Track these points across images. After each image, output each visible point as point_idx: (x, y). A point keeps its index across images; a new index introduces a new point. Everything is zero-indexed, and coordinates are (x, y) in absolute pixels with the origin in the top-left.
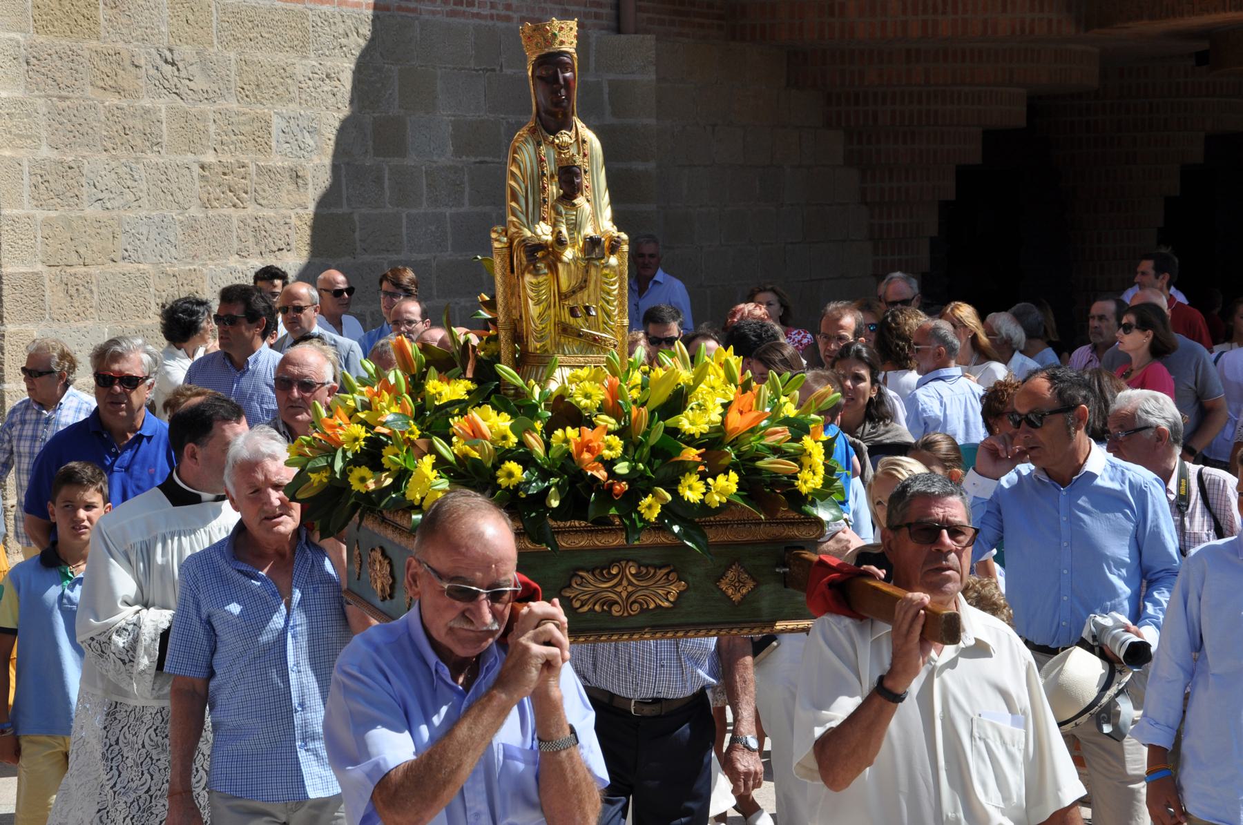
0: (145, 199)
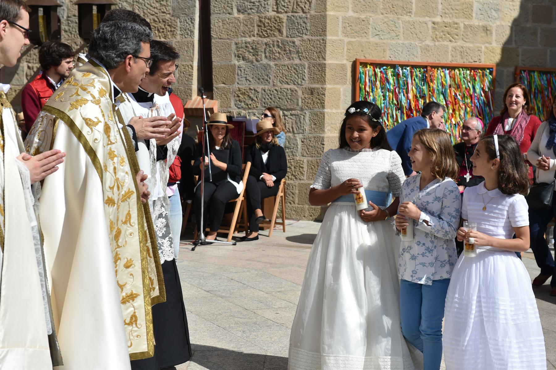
0: (401, 36)
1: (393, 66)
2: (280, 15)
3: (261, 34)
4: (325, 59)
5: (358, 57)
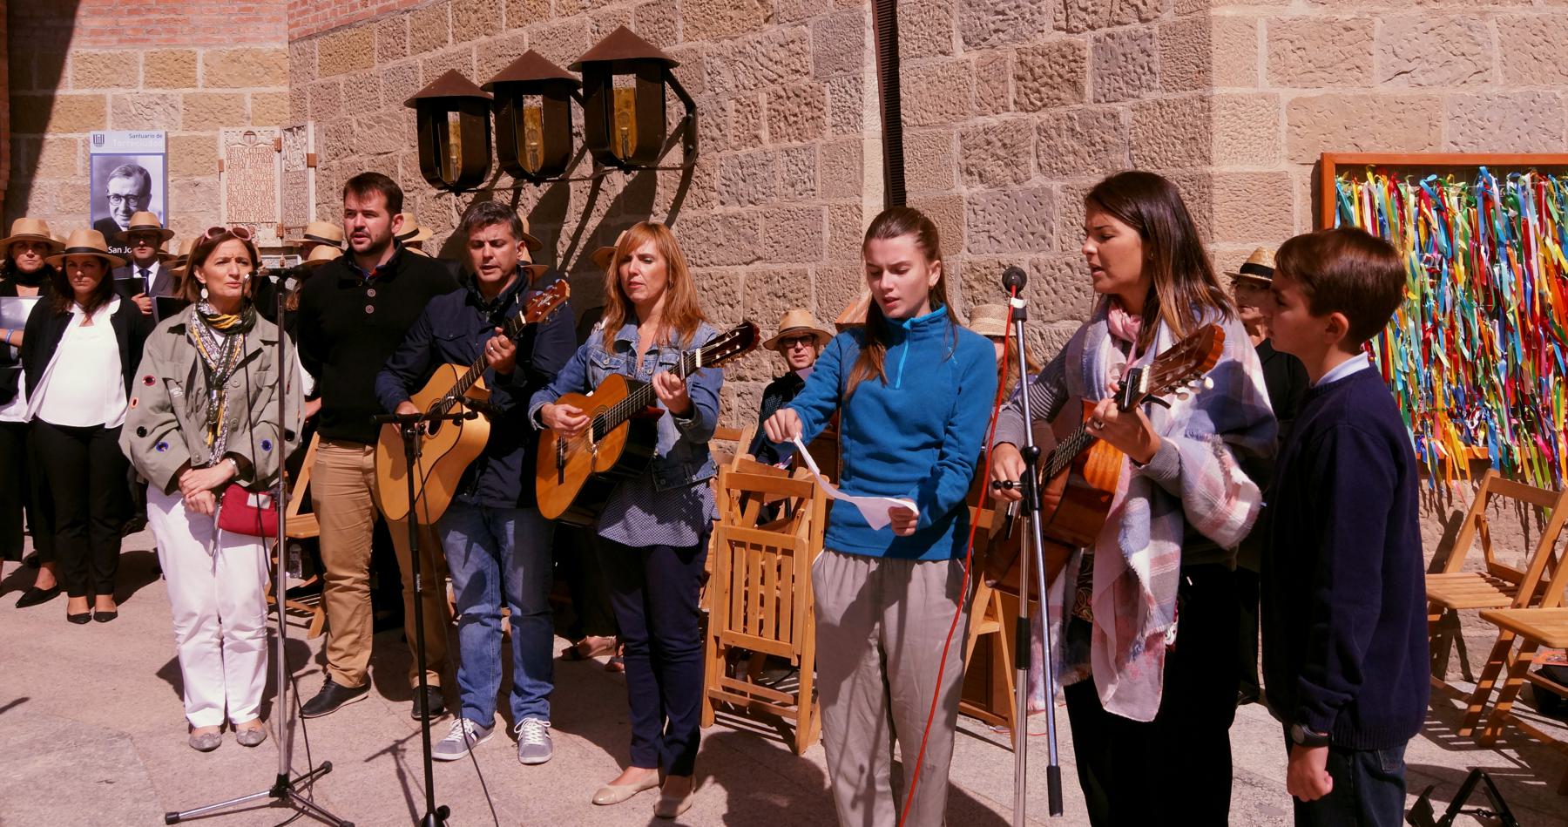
1: (1467, 172)
2: (1074, 38)
3: (1024, 100)
4: (1208, 160)
5: (1331, 148)
